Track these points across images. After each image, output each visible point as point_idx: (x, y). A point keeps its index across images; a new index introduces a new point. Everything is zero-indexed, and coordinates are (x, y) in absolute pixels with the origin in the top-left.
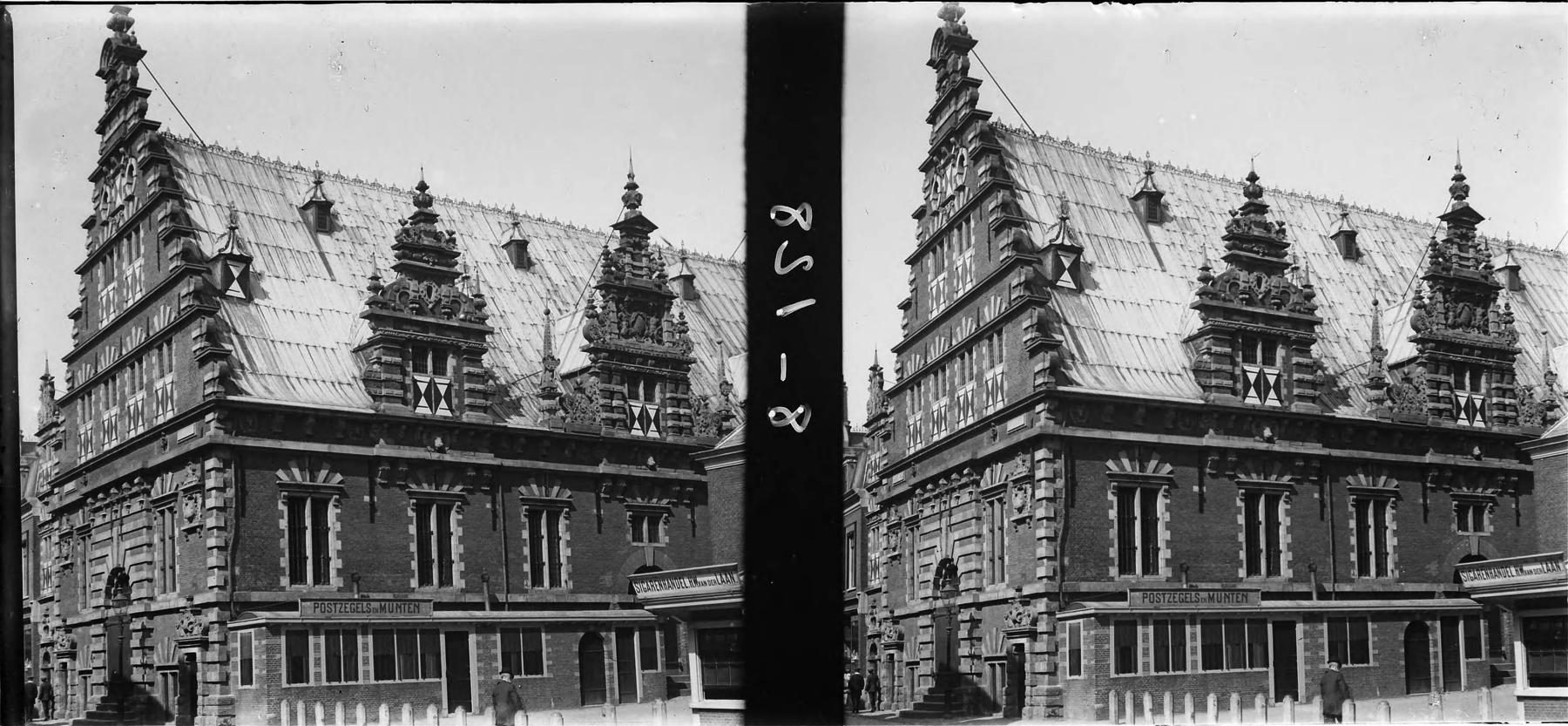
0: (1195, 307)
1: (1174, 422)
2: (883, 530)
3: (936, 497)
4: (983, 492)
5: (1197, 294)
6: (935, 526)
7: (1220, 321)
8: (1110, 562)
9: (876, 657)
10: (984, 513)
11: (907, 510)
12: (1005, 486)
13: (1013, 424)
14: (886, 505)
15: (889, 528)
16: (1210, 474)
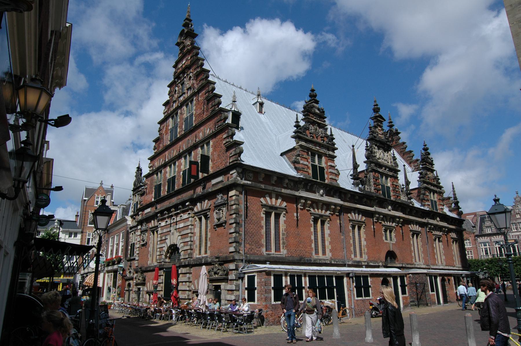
0: (293, 137)
1: (287, 184)
2: (139, 233)
3: (168, 217)
4: (195, 213)
5: (294, 132)
6: (168, 230)
7: (303, 143)
8: (262, 245)
9: (130, 289)
10: (196, 223)
11: (152, 224)
12: (209, 209)
13: (214, 181)
14: (140, 223)
15: (141, 232)
16: (300, 208)
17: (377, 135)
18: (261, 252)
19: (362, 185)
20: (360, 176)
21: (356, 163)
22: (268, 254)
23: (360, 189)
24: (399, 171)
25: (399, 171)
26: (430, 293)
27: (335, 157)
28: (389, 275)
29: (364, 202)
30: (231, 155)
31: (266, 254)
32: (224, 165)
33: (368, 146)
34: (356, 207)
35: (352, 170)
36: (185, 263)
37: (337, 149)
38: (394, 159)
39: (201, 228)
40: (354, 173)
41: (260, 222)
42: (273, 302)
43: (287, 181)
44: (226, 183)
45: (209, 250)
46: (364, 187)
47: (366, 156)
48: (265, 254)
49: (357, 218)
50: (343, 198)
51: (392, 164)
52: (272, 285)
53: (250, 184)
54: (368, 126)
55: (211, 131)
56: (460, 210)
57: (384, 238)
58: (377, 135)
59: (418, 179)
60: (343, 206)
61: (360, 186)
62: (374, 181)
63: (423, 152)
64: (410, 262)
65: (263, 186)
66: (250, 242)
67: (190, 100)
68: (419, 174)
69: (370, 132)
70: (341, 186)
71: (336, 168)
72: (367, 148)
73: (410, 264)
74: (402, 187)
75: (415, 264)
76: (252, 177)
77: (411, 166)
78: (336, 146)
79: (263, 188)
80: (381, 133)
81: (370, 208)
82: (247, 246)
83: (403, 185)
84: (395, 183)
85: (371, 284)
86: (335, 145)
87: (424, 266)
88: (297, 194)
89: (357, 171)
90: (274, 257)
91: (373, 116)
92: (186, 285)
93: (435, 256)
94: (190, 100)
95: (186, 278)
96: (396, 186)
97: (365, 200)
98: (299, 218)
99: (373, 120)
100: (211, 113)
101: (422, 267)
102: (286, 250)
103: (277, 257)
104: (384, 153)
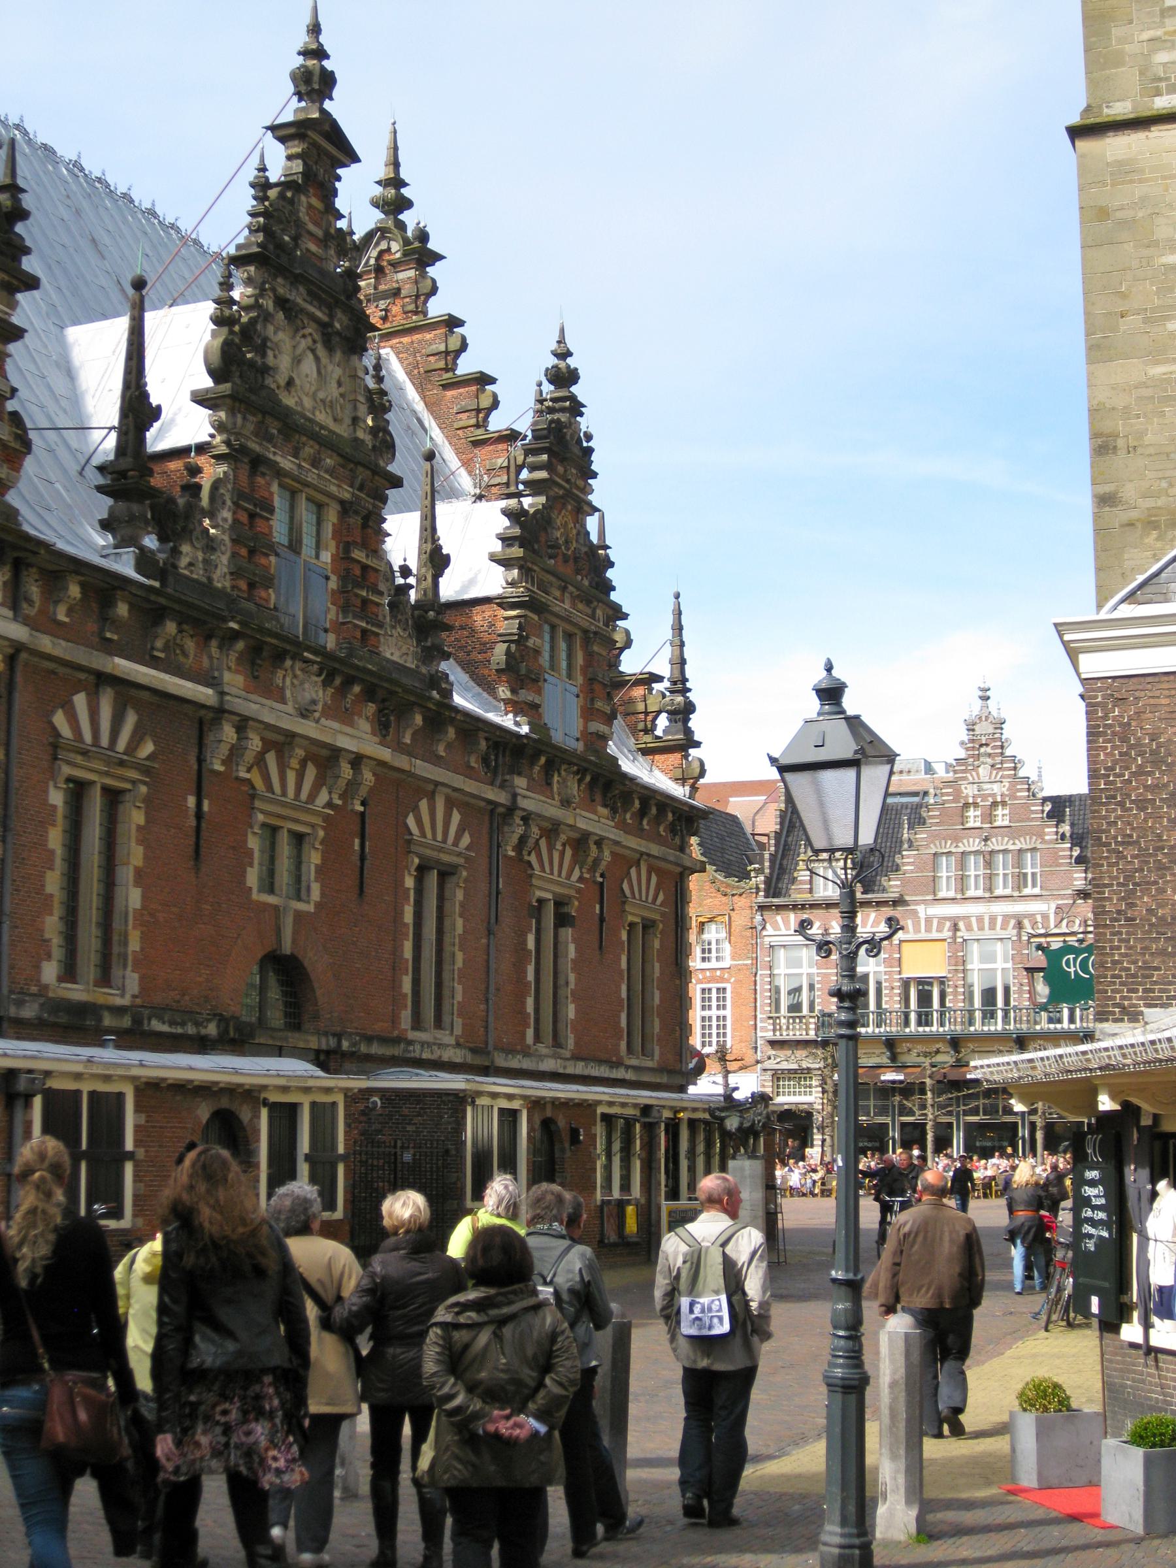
17: (296, 239)
19: (162, 539)
20: (156, 481)
21: (145, 396)
23: (144, 561)
24: (397, 482)
25: (397, 482)
27: (17, 333)
28: (251, 1095)
29: (159, 644)
33: (232, 302)
34: (108, 669)
35: (113, 436)
37: (31, 283)
38: (379, 402)
40: (120, 450)
46: (175, 552)
47: (216, 359)
49: (105, 741)
50: (30, 602)
51: (360, 434)
54: (250, 173)
56: (693, 752)
57: (252, 878)
58: (296, 239)
59: (498, 546)
60: (24, 656)
61: (150, 542)
62: (236, 521)
63: (547, 388)
64: (379, 1027)
68: (507, 522)
69: (253, 215)
70: (26, 528)
71: (11, 406)
72: (227, 312)
73: (384, 1040)
74: (400, 581)
75: (410, 1042)
77: (467, 464)
78: (29, 264)
80: (319, 233)
81: (189, 685)
83: (405, 571)
84: (358, 555)
85: (137, 1142)
86: (25, 259)
87: (457, 1056)
89: (141, 441)
91: (288, 117)
93: (524, 1003)
96: (365, 568)
97: (171, 627)
99: (282, 140)
101: (445, 1058)
104: (324, 360)
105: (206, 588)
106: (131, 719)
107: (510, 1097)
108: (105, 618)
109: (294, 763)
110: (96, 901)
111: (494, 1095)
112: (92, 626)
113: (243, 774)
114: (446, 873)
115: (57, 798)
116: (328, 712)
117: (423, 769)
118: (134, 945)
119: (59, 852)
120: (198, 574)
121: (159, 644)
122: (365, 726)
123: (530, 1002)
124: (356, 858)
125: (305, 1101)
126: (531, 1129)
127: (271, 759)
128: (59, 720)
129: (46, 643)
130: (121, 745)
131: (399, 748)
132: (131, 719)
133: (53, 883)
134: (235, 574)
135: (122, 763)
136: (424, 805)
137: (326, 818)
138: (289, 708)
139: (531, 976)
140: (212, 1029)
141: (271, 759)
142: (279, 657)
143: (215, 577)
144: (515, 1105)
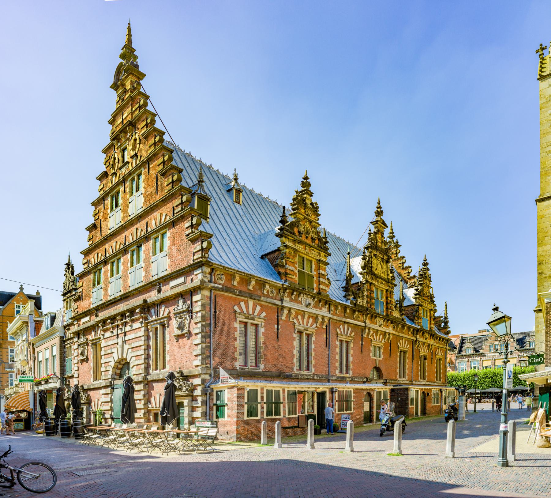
18: (234, 366)
22: (242, 369)
26: (410, 406)
30: (195, 251)
31: (239, 368)
32: (185, 264)
36: (138, 379)
39: (156, 340)
41: (233, 333)
42: (246, 418)
43: (267, 287)
44: (189, 285)
45: (168, 364)
48: (238, 368)
52: (246, 401)
53: (220, 288)
55: (168, 219)
65: (238, 292)
66: (220, 355)
67: (137, 173)
76: (224, 280)
79: (238, 293)
82: (217, 359)
88: (279, 303)
90: (249, 371)
92: (141, 403)
94: (137, 173)
95: (140, 395)
97: (357, 313)
98: (280, 330)
100: (167, 192)
102: (263, 365)
103: (252, 371)
105: (362, 306)
106: (350, 329)
107: (417, 388)
108: (345, 312)
109: (378, 335)
110: (345, 360)
111: (414, 388)
112: (343, 314)
113: (370, 337)
114: (405, 352)
115: (338, 343)
116: (384, 326)
117: (401, 334)
118: (351, 366)
119: (338, 352)
120: (361, 304)
121: (355, 316)
122: (390, 328)
123: (419, 373)
124: (389, 350)
125: (382, 390)
126: (421, 393)
127: (374, 334)
128: (338, 330)
129: (335, 317)
130: (349, 334)
131: (396, 331)
132: (350, 329)
133: (338, 357)
134: (367, 303)
135: (349, 337)
136: (401, 341)
137: (384, 344)
138: (378, 326)
139: (419, 368)
140: (365, 380)
141: (374, 334)
142: (376, 317)
143: (364, 304)
144: (418, 389)
